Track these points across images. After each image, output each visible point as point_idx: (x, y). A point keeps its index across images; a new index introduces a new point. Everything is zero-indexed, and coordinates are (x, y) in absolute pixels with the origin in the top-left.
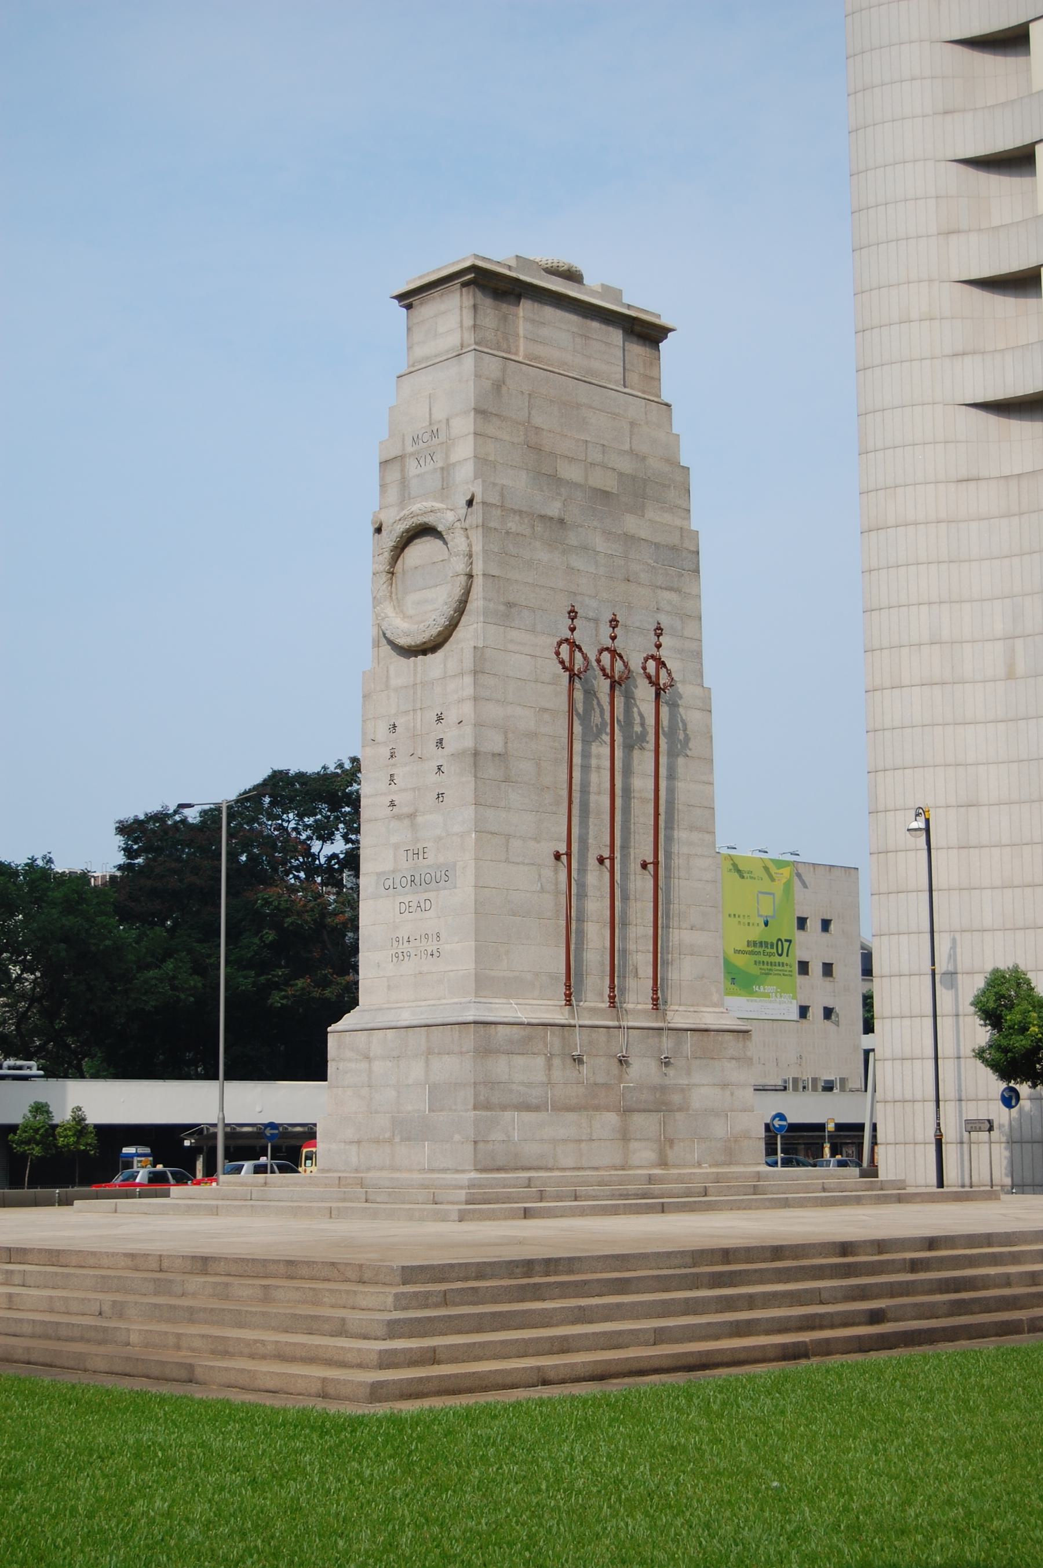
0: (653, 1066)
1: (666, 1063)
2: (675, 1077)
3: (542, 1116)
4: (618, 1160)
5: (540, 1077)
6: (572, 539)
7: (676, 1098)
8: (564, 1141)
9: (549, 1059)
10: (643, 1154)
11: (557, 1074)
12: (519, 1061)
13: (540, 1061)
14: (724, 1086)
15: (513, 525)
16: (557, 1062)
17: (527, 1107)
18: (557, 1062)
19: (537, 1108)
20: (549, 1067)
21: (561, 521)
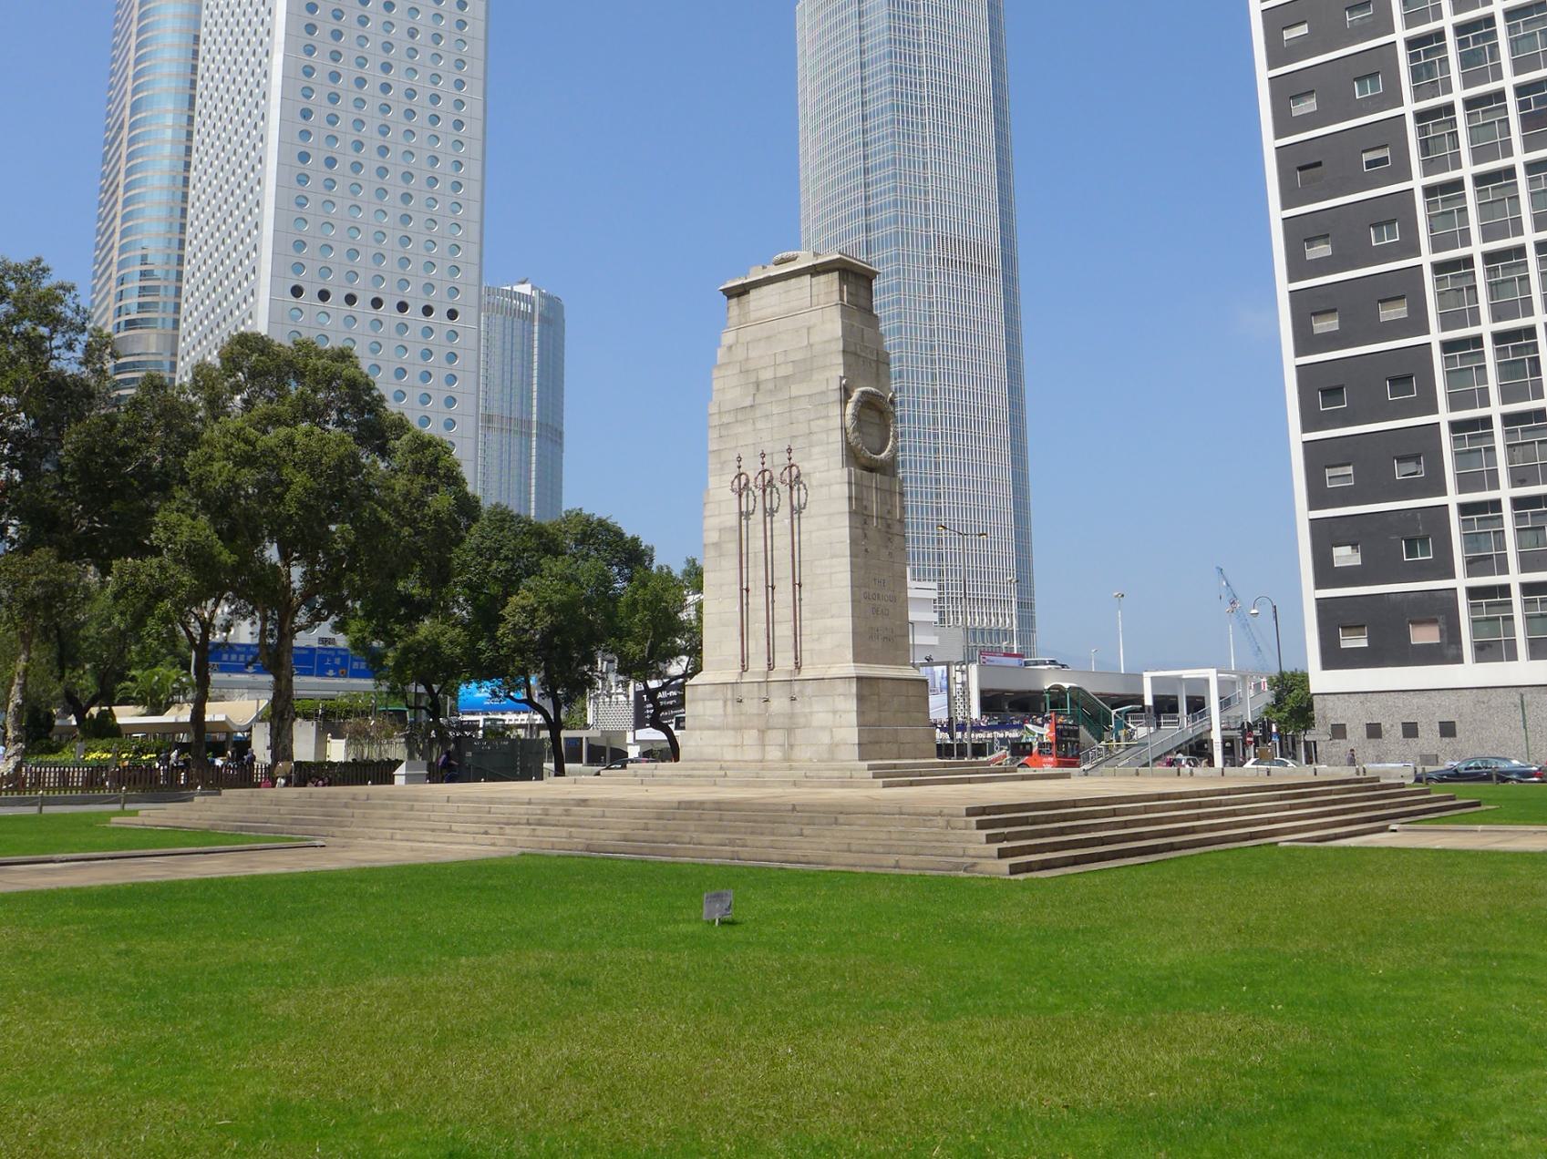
0: (786, 701)
1: (793, 699)
2: (797, 705)
3: (717, 732)
4: (758, 757)
5: (721, 711)
6: (758, 413)
7: (802, 721)
8: (730, 746)
9: (725, 702)
10: (774, 753)
11: (729, 709)
12: (709, 704)
13: (720, 703)
14: (835, 712)
15: (726, 419)
16: (729, 703)
17: (713, 728)
18: (729, 703)
19: (718, 728)
20: (725, 705)
21: (752, 406)
